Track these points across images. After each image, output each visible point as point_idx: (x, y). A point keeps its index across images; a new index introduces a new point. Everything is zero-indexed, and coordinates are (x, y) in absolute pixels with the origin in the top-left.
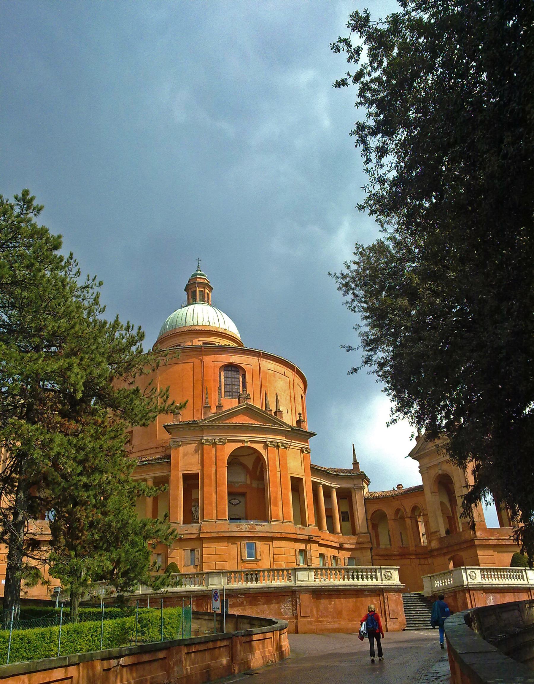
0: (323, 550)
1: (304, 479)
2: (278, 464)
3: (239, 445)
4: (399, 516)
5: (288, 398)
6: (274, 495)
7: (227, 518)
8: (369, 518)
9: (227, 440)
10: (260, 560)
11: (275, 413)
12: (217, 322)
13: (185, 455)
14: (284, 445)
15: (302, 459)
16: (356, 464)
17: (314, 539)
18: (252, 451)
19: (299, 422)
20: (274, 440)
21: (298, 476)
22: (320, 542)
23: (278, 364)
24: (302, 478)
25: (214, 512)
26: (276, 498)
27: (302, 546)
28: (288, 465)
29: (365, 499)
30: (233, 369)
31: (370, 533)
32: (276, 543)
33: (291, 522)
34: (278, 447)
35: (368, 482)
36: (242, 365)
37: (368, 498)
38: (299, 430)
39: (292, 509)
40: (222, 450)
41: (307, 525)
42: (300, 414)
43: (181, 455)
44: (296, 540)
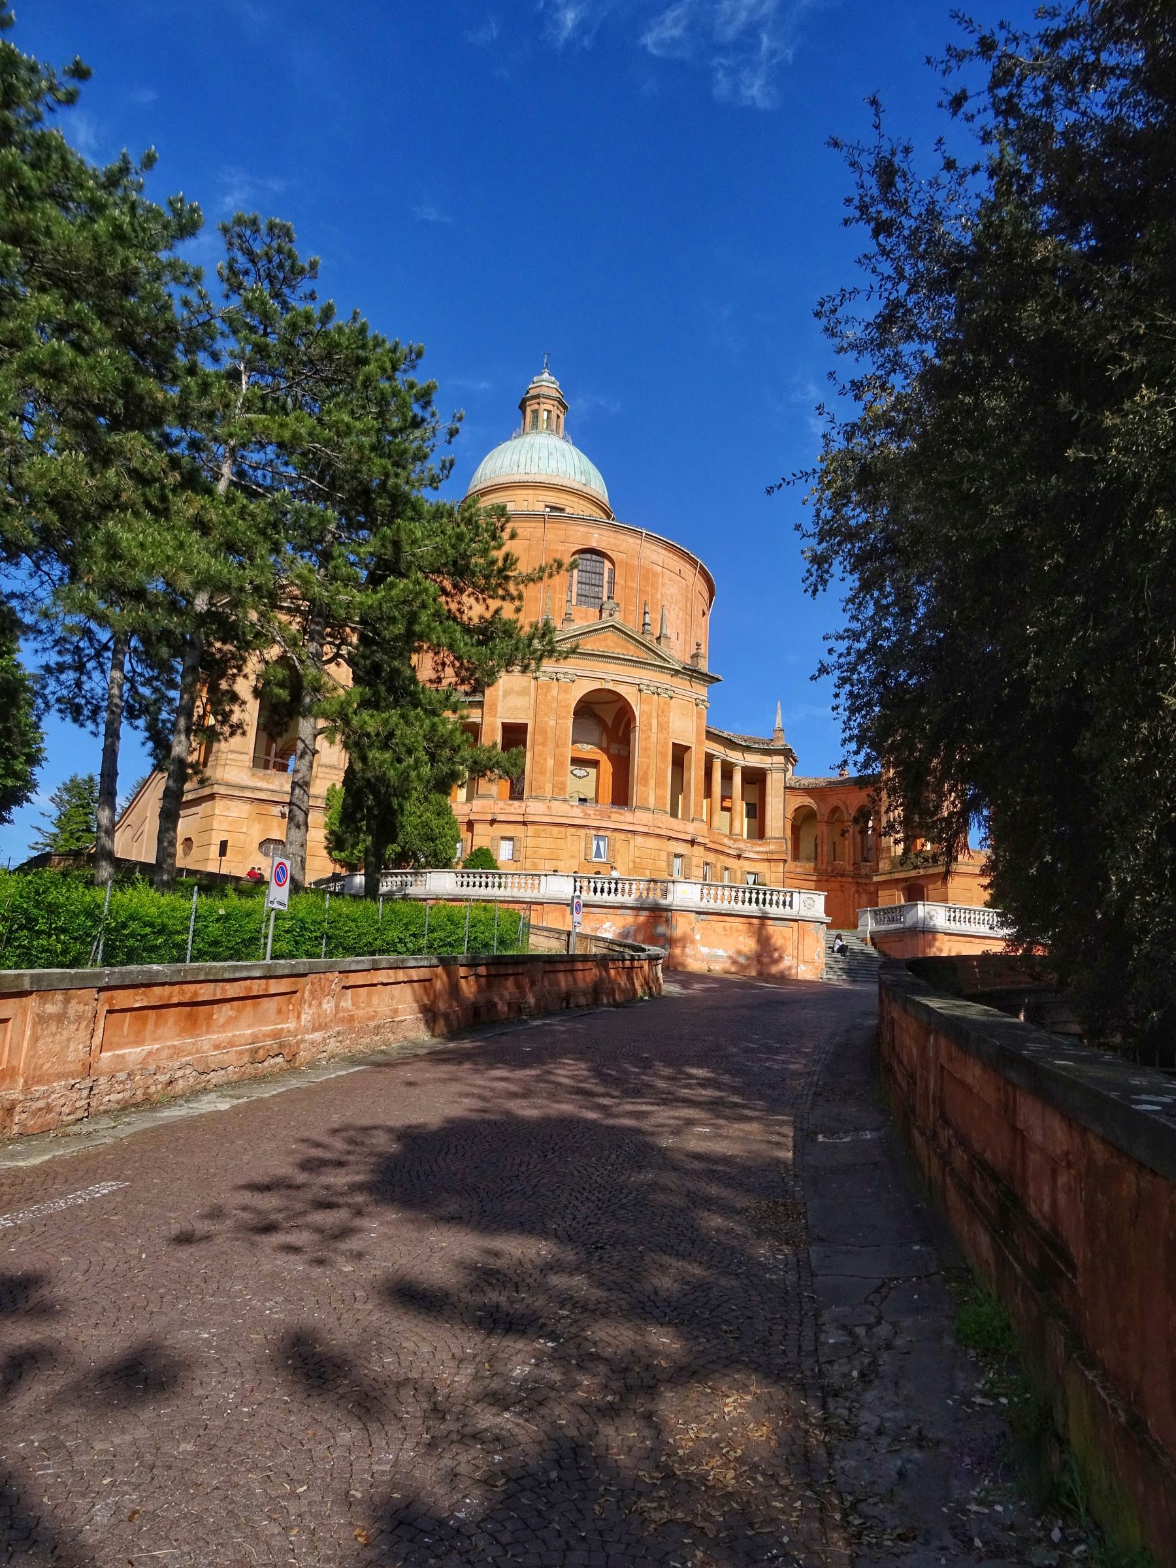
0: (711, 857)
1: (693, 749)
2: (654, 722)
3: (596, 685)
5: (681, 614)
11: (658, 639)
12: (571, 470)
13: (506, 693)
17: (699, 840)
18: (613, 698)
19: (695, 656)
20: (652, 684)
23: (671, 555)
24: (689, 748)
25: (549, 787)
26: (646, 773)
27: (681, 848)
30: (594, 557)
32: (639, 840)
33: (665, 812)
36: (609, 553)
38: (694, 671)
40: (566, 691)
42: (698, 645)
43: (501, 693)
44: (670, 838)
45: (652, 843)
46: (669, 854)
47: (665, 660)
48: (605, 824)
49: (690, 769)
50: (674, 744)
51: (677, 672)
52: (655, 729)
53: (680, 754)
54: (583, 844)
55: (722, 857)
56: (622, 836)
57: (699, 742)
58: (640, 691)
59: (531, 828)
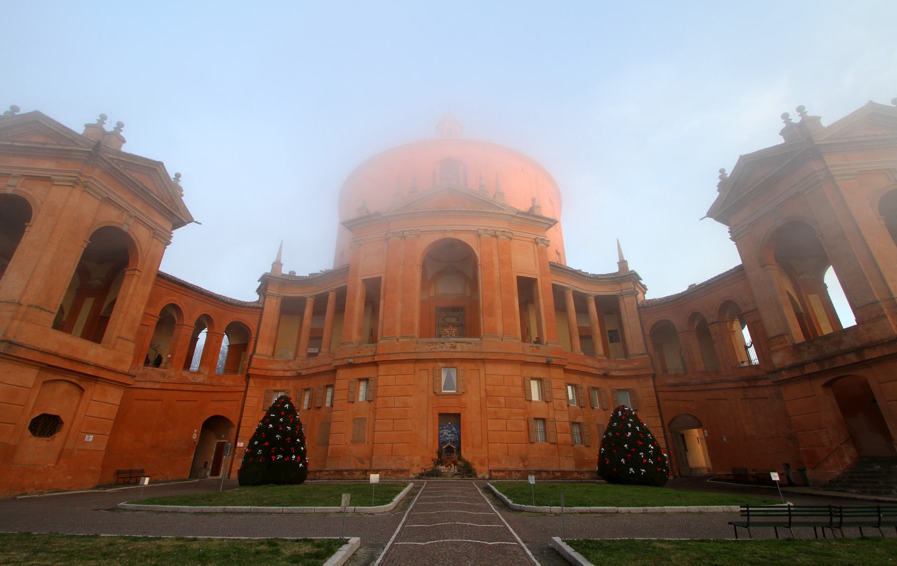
0: (575, 379)
1: (539, 280)
3: (438, 237)
4: (696, 325)
7: (416, 334)
8: (647, 332)
9: (420, 231)
10: (463, 393)
14: (507, 234)
15: (537, 255)
16: (623, 264)
17: (554, 361)
20: (490, 229)
21: (529, 276)
22: (566, 367)
24: (536, 279)
27: (538, 372)
28: (513, 261)
29: (639, 308)
31: (650, 355)
32: (490, 368)
35: (644, 289)
37: (644, 307)
41: (545, 343)
44: (525, 363)
47: (499, 208)
49: (538, 298)
52: (496, 265)
54: (431, 377)
55: (587, 378)
56: (471, 366)
59: (382, 369)
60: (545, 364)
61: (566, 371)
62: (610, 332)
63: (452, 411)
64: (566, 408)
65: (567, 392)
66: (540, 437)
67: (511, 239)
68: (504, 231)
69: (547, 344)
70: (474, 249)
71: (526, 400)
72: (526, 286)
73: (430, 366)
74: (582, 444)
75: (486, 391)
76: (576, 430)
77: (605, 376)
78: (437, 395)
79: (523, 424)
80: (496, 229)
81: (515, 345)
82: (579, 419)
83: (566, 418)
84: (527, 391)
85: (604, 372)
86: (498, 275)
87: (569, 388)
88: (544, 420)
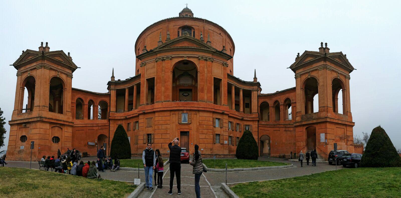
0: (232, 120)
2: (206, 70)
6: (202, 86)
10: (191, 123)
15: (223, 70)
17: (226, 113)
20: (204, 56)
22: (229, 115)
24: (221, 80)
27: (219, 116)
28: (213, 71)
32: (201, 114)
34: (206, 60)
39: (213, 95)
41: (223, 105)
44: (214, 112)
45: (206, 114)
46: (213, 119)
48: (185, 108)
50: (214, 78)
51: (214, 52)
52: (206, 72)
53: (217, 82)
54: (177, 117)
55: (236, 120)
56: (194, 113)
57: (225, 78)
58: (199, 59)
60: (221, 113)
61: (229, 117)
62: (246, 103)
63: (186, 130)
64: (228, 131)
65: (228, 124)
66: (218, 141)
67: (212, 62)
68: (210, 58)
69: (223, 105)
70: (197, 65)
71: (214, 127)
72: (217, 82)
73: (177, 113)
74: (231, 144)
75: (199, 122)
76: (230, 139)
77: (242, 120)
78: (180, 124)
79: (212, 136)
80: (206, 57)
81: (211, 105)
82: (231, 135)
83: (227, 134)
84: (214, 123)
85: (242, 118)
86: (206, 76)
87: (229, 123)
88: (219, 135)
